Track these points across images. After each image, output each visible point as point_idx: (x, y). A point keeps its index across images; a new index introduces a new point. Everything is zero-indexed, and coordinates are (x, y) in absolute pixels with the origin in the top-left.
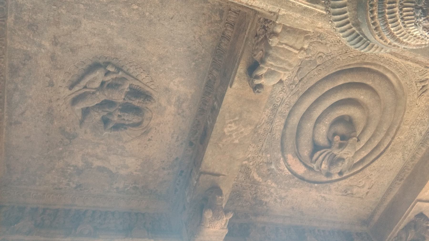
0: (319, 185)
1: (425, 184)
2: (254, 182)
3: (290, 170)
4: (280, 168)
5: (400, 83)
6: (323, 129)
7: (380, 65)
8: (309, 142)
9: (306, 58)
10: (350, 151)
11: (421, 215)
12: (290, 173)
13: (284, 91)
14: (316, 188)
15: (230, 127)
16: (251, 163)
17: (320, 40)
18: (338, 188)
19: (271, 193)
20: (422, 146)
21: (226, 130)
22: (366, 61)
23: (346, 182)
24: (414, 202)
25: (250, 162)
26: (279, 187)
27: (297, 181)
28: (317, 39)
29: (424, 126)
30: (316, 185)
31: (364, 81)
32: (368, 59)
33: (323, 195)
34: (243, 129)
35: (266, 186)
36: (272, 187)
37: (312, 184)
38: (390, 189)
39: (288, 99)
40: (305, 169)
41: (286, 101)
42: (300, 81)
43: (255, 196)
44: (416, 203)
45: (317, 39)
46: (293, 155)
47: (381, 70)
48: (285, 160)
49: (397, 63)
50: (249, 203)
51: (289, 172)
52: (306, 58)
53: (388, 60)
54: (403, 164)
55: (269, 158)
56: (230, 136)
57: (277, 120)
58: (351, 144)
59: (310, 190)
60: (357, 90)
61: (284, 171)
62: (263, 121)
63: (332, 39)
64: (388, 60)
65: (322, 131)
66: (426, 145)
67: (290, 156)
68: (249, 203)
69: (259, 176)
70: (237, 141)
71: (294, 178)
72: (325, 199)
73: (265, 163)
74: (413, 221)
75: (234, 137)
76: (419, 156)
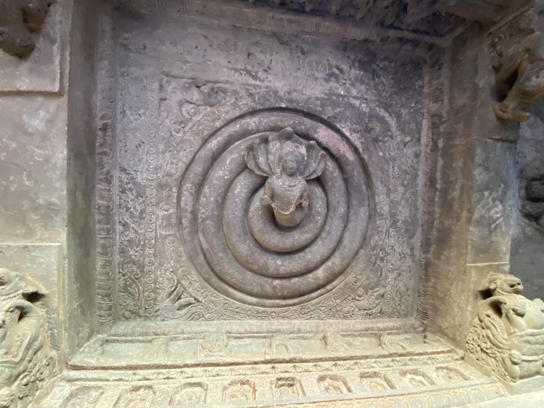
0: (277, 105)
1: (68, 140)
2: (387, 107)
3: (338, 131)
4: (358, 135)
5: (227, 294)
6: (319, 206)
7: (272, 307)
8: (333, 184)
9: (378, 291)
10: (288, 193)
11: (22, 53)
12: (338, 125)
13: (390, 248)
14: (281, 100)
15: (497, 213)
16: (399, 139)
17: (368, 312)
18: (236, 99)
19: (353, 85)
20: (108, 207)
21: (500, 207)
22: (298, 307)
23: (227, 113)
24: (67, 89)
25: (400, 141)
26: (346, 99)
27: (320, 112)
28: (372, 312)
29: (128, 241)
30: (283, 105)
31: (285, 282)
32: (296, 311)
33: (258, 83)
34: (483, 212)
35: (366, 99)
36: (356, 98)
37: (290, 106)
38: (112, 101)
39: (383, 238)
40: (316, 136)
41: (384, 235)
42: (375, 263)
43: (377, 80)
44: (61, 87)
45: (372, 312)
46: (347, 159)
47: (268, 302)
48: (355, 150)
49: (248, 318)
50: (381, 65)
51: (341, 128)
52: (378, 291)
53: (266, 317)
54: (119, 160)
55: (379, 149)
56: (494, 200)
57: (386, 208)
58: (291, 204)
59: (289, 93)
60: (294, 271)
61: (350, 129)
62: (402, 203)
63: (355, 318)
64: (266, 317)
65: (320, 205)
66: (104, 212)
67: (350, 156)
68: (381, 65)
69: (383, 118)
70: (487, 193)
71: (329, 117)
72: (249, 72)
73: (381, 141)
74: (35, 30)
75: (490, 200)
76: (100, 187)
